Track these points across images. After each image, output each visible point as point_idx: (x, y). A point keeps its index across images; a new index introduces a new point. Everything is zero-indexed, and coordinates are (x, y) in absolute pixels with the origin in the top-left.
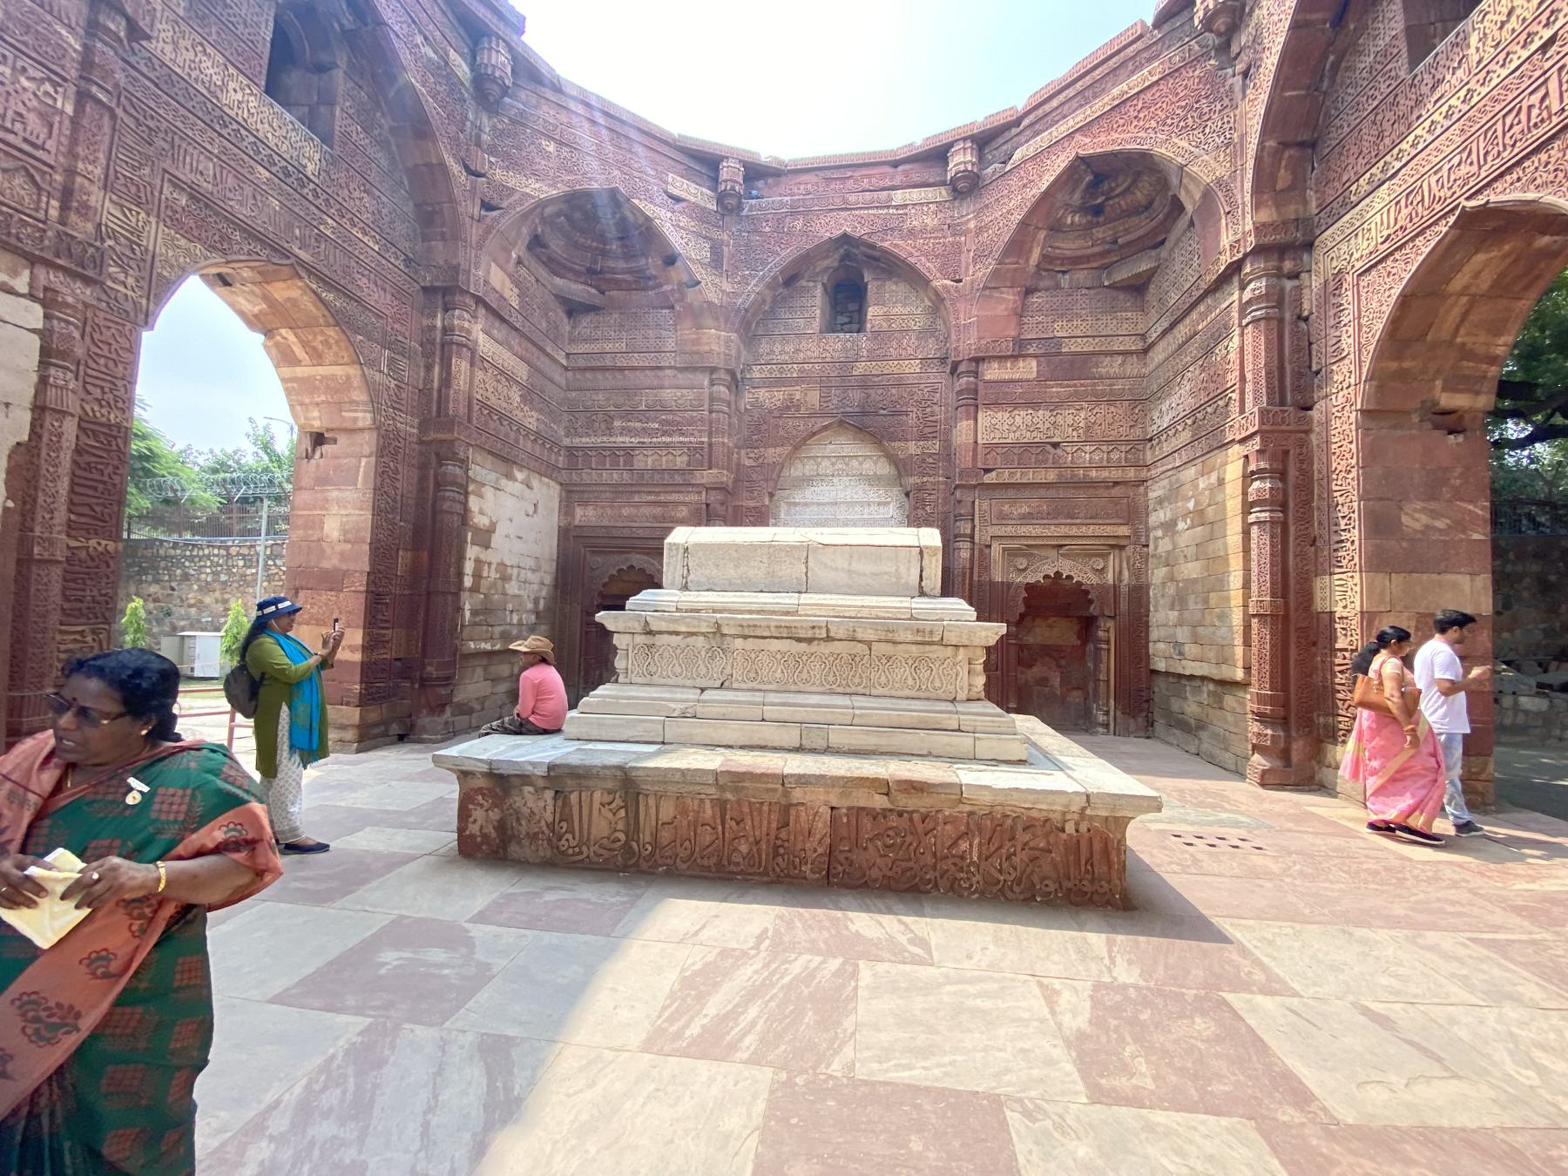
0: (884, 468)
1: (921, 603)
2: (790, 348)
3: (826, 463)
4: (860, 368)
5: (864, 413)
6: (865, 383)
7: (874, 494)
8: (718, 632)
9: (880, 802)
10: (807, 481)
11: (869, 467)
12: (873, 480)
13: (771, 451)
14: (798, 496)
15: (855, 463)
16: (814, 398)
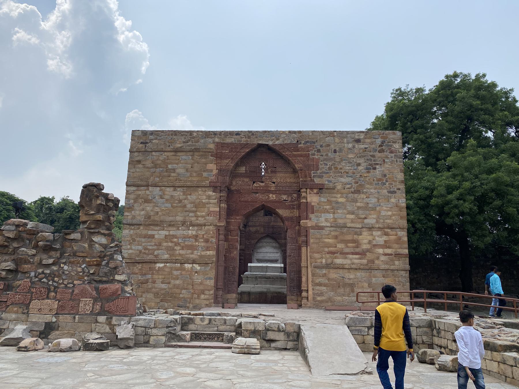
0: (277, 245)
1: (281, 274)
2: (257, 219)
3: (265, 243)
4: (272, 224)
5: (273, 233)
6: (273, 227)
7: (275, 251)
8: (256, 278)
9: (276, 295)
10: (261, 247)
11: (274, 244)
12: (275, 248)
13: (253, 241)
14: (259, 251)
15: (271, 244)
16: (262, 230)
